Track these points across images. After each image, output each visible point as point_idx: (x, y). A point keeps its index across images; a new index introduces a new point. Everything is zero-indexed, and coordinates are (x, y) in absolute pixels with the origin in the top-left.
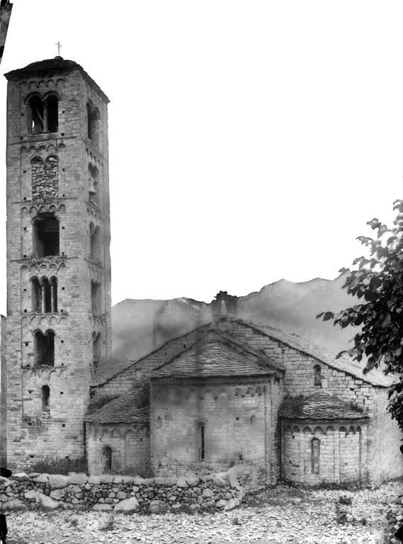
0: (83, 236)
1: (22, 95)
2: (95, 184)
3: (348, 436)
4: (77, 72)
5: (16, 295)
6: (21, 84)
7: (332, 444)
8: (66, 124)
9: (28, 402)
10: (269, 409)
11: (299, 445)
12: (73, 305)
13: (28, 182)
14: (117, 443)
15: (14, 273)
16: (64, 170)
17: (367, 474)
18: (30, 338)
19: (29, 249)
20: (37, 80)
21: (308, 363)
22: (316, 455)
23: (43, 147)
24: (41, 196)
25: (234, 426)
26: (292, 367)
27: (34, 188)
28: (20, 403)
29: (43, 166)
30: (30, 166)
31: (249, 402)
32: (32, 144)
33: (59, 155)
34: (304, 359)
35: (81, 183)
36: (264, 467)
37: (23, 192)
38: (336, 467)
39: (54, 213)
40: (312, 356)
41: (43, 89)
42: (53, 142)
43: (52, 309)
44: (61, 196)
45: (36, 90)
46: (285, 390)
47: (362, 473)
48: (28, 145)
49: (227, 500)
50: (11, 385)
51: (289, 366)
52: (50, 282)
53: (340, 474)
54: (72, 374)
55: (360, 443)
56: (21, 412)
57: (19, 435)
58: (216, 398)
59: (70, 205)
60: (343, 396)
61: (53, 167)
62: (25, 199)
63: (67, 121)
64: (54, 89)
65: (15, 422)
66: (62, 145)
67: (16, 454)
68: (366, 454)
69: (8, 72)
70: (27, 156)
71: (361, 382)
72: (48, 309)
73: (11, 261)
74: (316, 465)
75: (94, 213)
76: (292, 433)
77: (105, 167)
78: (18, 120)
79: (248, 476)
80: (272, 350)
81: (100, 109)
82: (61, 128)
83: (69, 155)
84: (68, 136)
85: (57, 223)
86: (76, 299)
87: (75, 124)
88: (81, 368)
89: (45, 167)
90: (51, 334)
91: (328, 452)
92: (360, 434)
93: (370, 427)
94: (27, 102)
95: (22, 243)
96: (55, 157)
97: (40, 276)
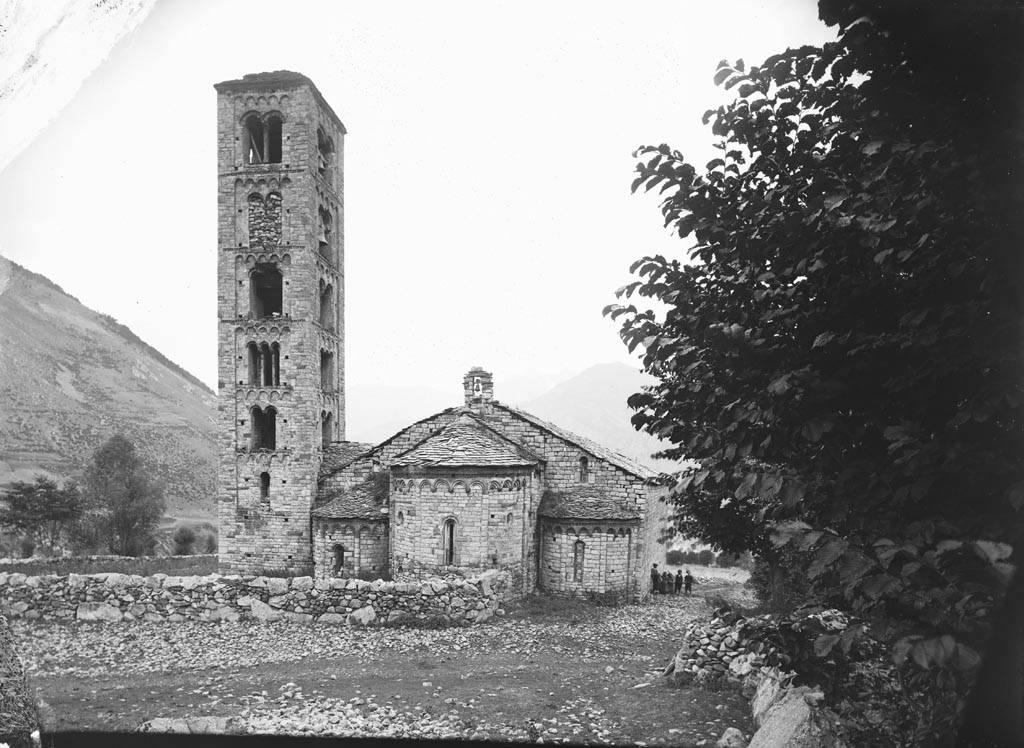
0: (312, 294)
1: (238, 113)
2: (327, 232)
3: (617, 539)
4: (306, 87)
6: (236, 99)
7: (598, 548)
8: (292, 153)
9: (243, 491)
10: (528, 506)
11: (561, 548)
13: (244, 224)
14: (348, 541)
16: (288, 211)
17: (635, 582)
18: (246, 415)
19: (246, 308)
20: (257, 95)
21: (573, 454)
22: (579, 561)
23: (262, 181)
24: (260, 242)
25: (489, 524)
26: (554, 459)
27: (252, 232)
28: (234, 492)
29: (262, 205)
30: (247, 204)
31: (507, 497)
32: (250, 176)
33: (283, 192)
34: (569, 450)
35: (308, 227)
36: (520, 572)
37: (239, 237)
38: (602, 574)
39: (276, 264)
40: (578, 446)
41: (263, 108)
42: (276, 175)
43: (274, 383)
44: (284, 243)
45: (255, 108)
46: (546, 485)
47: (630, 581)
48: (244, 177)
49: (479, 610)
51: (551, 457)
52: (271, 349)
53: (606, 582)
54: (297, 460)
55: (629, 547)
58: (468, 492)
59: (296, 256)
60: (612, 493)
61: (275, 206)
62: (240, 245)
63: (292, 150)
64: (277, 108)
66: (287, 180)
68: (635, 560)
69: (219, 81)
70: (243, 191)
71: (633, 478)
72: (268, 382)
73: (223, 321)
74: (579, 571)
75: (326, 268)
76: (553, 534)
77: (340, 210)
78: (232, 145)
79: (502, 582)
80: (532, 439)
81: (334, 139)
82: (286, 159)
83: (295, 192)
84: (294, 168)
85: (280, 277)
86: (302, 371)
87: (303, 153)
88: (307, 453)
89: (266, 206)
90: (272, 411)
91: (593, 557)
92: (630, 537)
93: (641, 529)
94: (244, 123)
95: (236, 300)
96: (278, 194)
97: (258, 341)
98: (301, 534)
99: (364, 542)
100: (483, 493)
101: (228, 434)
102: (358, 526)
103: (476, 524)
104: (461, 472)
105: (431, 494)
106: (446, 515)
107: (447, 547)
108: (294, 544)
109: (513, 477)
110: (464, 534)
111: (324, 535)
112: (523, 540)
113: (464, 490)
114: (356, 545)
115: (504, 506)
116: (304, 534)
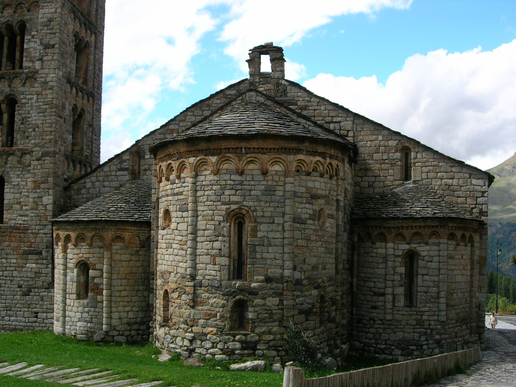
3: (459, 248)
7: (436, 259)
12: (45, 58)
47: (474, 305)
52: (16, 28)
54: (38, 160)
58: (265, 173)
86: (50, 50)
92: (472, 246)
98: (40, 253)
99: (117, 257)
100: (286, 175)
102: (109, 234)
103: (276, 222)
104: (254, 144)
106: (233, 207)
107: (235, 254)
108: (31, 265)
109: (324, 158)
112: (337, 249)
113: (259, 172)
115: (314, 197)
116: (44, 253)
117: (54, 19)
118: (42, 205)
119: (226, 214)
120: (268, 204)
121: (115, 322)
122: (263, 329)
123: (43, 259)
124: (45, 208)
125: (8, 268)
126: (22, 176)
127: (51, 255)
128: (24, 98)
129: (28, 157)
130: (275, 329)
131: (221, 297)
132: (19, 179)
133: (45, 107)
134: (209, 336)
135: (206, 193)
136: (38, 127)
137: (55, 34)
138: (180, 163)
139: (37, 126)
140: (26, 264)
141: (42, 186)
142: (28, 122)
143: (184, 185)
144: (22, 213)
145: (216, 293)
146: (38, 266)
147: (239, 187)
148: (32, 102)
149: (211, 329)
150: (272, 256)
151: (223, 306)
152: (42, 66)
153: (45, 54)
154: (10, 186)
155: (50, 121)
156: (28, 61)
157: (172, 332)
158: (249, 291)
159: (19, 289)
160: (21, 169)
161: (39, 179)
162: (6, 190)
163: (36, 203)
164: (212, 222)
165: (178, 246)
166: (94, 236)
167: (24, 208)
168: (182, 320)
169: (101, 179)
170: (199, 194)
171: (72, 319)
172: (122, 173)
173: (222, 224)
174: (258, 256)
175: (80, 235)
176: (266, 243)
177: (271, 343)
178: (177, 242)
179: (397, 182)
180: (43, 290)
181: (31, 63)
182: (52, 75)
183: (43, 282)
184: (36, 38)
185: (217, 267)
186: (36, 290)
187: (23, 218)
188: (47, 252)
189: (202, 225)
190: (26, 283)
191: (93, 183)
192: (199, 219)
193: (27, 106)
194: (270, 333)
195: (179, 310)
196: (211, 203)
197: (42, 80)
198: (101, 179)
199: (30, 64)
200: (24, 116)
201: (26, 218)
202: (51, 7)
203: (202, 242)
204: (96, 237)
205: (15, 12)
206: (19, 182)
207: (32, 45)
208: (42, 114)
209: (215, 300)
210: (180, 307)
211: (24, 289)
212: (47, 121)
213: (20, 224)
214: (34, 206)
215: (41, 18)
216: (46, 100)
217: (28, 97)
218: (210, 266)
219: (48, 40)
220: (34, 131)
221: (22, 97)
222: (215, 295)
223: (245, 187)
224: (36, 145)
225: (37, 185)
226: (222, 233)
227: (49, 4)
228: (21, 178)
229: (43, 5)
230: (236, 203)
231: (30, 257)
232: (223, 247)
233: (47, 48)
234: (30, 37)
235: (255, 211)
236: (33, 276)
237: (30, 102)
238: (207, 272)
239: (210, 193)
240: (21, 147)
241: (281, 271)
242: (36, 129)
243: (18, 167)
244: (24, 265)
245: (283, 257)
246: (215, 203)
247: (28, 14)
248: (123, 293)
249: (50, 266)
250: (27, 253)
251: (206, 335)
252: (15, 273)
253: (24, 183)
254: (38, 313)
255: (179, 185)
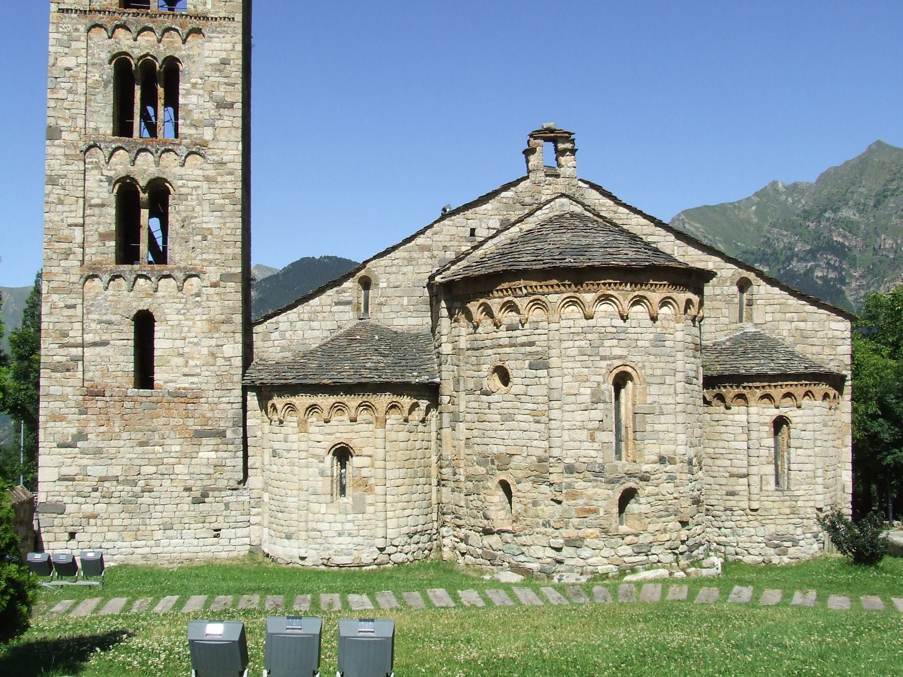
5: (70, 91)
12: (218, 123)
15: (71, 39)
50: (53, 307)
54: (214, 285)
56: (79, 374)
57: (74, 431)
65: (63, 398)
67: (64, 478)
99: (393, 436)
101: (66, 232)
103: (669, 380)
105: (585, 323)
108: (207, 453)
110: (649, 399)
111: (303, 426)
114: (380, 442)
116: (229, 434)
117: (232, 61)
118: (224, 358)
119: (607, 372)
120: (658, 359)
121: (391, 533)
122: (659, 526)
123: (227, 444)
124: (228, 363)
125: (165, 461)
126: (185, 311)
127: (242, 436)
128: (183, 186)
129: (195, 279)
130: (671, 525)
131: (604, 485)
132: (181, 317)
133: (222, 201)
134: (588, 540)
135: (577, 343)
136: (211, 234)
137: (233, 85)
138: (530, 302)
139: (209, 232)
140: (198, 452)
141: (224, 327)
142: (194, 225)
143: (537, 332)
144: (186, 370)
145: (597, 481)
146: (220, 454)
147: (622, 336)
148: (200, 192)
149: (591, 531)
150: (664, 428)
151: (608, 498)
152: (215, 135)
153: (219, 117)
154: (164, 328)
155: (232, 225)
156: (187, 126)
157: (523, 539)
158: (640, 475)
159: (187, 494)
160: (183, 301)
161: (217, 317)
162: (156, 335)
163: (213, 355)
164: (587, 384)
165: (531, 419)
166: (359, 406)
167: (191, 363)
168: (541, 521)
169: (306, 317)
170: (565, 344)
171: (324, 534)
172: (341, 308)
173: (603, 387)
174: (648, 428)
175: (336, 405)
176: (657, 411)
177: (667, 544)
178: (529, 412)
179: (733, 326)
180: (229, 492)
181: (193, 128)
182: (231, 152)
183: (229, 480)
184: (199, 89)
185: (596, 445)
186: (216, 493)
187: (189, 378)
188: (234, 432)
189: (572, 387)
190: (199, 483)
191: (291, 323)
192: (565, 380)
193: (189, 199)
194: (665, 531)
195: (534, 508)
196: (586, 358)
197: (215, 157)
198: (306, 317)
199: (193, 131)
200: (184, 215)
201: (195, 379)
202: (224, 40)
203: (573, 412)
204: (362, 408)
205: (159, 41)
206: (180, 321)
207: (193, 99)
208: (219, 214)
209: (597, 490)
210: (535, 503)
211: (198, 494)
212: (228, 225)
213: (184, 389)
214: (211, 360)
215: (208, 57)
216: (224, 191)
217: (190, 184)
218: (587, 445)
219: (223, 94)
220: (205, 238)
221: (180, 183)
222: (595, 484)
223: (630, 335)
224: (210, 262)
225: (214, 325)
226: (602, 398)
227: (221, 35)
228: (184, 314)
229: (210, 35)
230: (620, 357)
231: (204, 441)
232: (605, 417)
233: (221, 107)
234: (188, 86)
235: (644, 367)
236: (211, 471)
237: (194, 193)
238: (582, 453)
239: (583, 343)
240: (182, 264)
241: (673, 447)
242: (210, 237)
243: (178, 298)
244: (194, 455)
245: (675, 429)
246: (591, 358)
247: (183, 47)
248: (402, 489)
249: (240, 454)
250: (199, 435)
251: (582, 539)
252: (179, 469)
253: (190, 323)
254: (220, 530)
255: (527, 332)
